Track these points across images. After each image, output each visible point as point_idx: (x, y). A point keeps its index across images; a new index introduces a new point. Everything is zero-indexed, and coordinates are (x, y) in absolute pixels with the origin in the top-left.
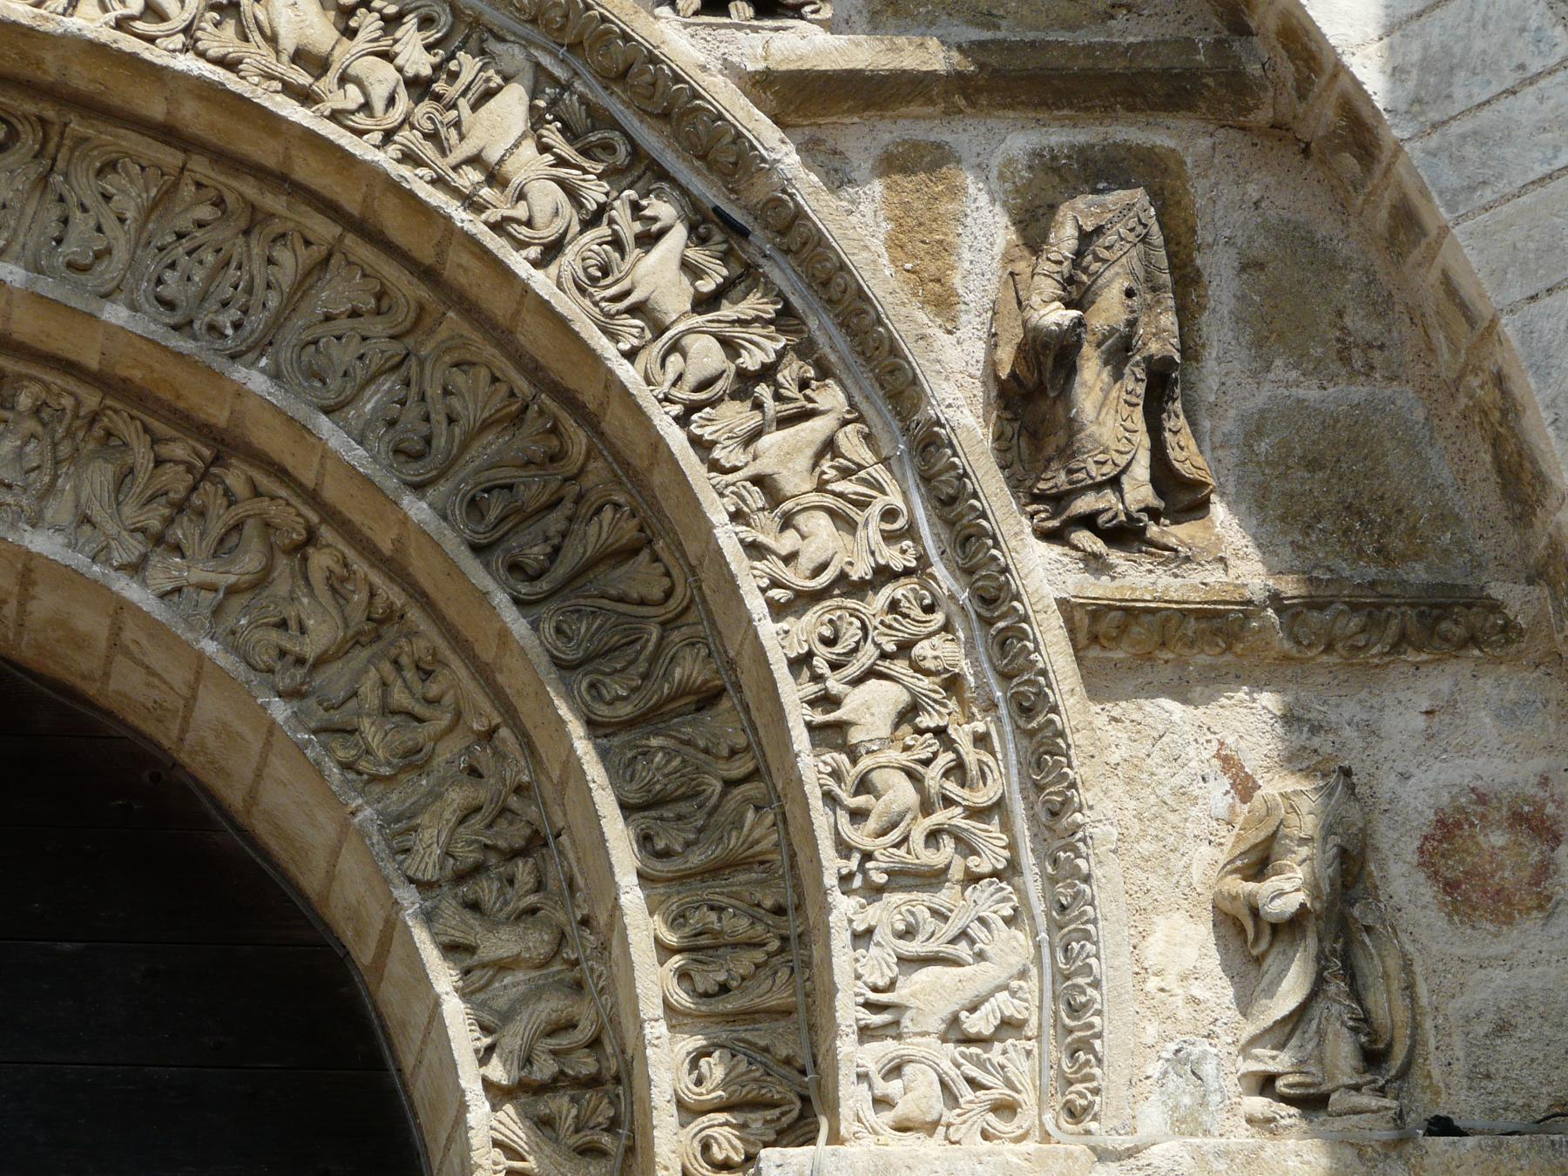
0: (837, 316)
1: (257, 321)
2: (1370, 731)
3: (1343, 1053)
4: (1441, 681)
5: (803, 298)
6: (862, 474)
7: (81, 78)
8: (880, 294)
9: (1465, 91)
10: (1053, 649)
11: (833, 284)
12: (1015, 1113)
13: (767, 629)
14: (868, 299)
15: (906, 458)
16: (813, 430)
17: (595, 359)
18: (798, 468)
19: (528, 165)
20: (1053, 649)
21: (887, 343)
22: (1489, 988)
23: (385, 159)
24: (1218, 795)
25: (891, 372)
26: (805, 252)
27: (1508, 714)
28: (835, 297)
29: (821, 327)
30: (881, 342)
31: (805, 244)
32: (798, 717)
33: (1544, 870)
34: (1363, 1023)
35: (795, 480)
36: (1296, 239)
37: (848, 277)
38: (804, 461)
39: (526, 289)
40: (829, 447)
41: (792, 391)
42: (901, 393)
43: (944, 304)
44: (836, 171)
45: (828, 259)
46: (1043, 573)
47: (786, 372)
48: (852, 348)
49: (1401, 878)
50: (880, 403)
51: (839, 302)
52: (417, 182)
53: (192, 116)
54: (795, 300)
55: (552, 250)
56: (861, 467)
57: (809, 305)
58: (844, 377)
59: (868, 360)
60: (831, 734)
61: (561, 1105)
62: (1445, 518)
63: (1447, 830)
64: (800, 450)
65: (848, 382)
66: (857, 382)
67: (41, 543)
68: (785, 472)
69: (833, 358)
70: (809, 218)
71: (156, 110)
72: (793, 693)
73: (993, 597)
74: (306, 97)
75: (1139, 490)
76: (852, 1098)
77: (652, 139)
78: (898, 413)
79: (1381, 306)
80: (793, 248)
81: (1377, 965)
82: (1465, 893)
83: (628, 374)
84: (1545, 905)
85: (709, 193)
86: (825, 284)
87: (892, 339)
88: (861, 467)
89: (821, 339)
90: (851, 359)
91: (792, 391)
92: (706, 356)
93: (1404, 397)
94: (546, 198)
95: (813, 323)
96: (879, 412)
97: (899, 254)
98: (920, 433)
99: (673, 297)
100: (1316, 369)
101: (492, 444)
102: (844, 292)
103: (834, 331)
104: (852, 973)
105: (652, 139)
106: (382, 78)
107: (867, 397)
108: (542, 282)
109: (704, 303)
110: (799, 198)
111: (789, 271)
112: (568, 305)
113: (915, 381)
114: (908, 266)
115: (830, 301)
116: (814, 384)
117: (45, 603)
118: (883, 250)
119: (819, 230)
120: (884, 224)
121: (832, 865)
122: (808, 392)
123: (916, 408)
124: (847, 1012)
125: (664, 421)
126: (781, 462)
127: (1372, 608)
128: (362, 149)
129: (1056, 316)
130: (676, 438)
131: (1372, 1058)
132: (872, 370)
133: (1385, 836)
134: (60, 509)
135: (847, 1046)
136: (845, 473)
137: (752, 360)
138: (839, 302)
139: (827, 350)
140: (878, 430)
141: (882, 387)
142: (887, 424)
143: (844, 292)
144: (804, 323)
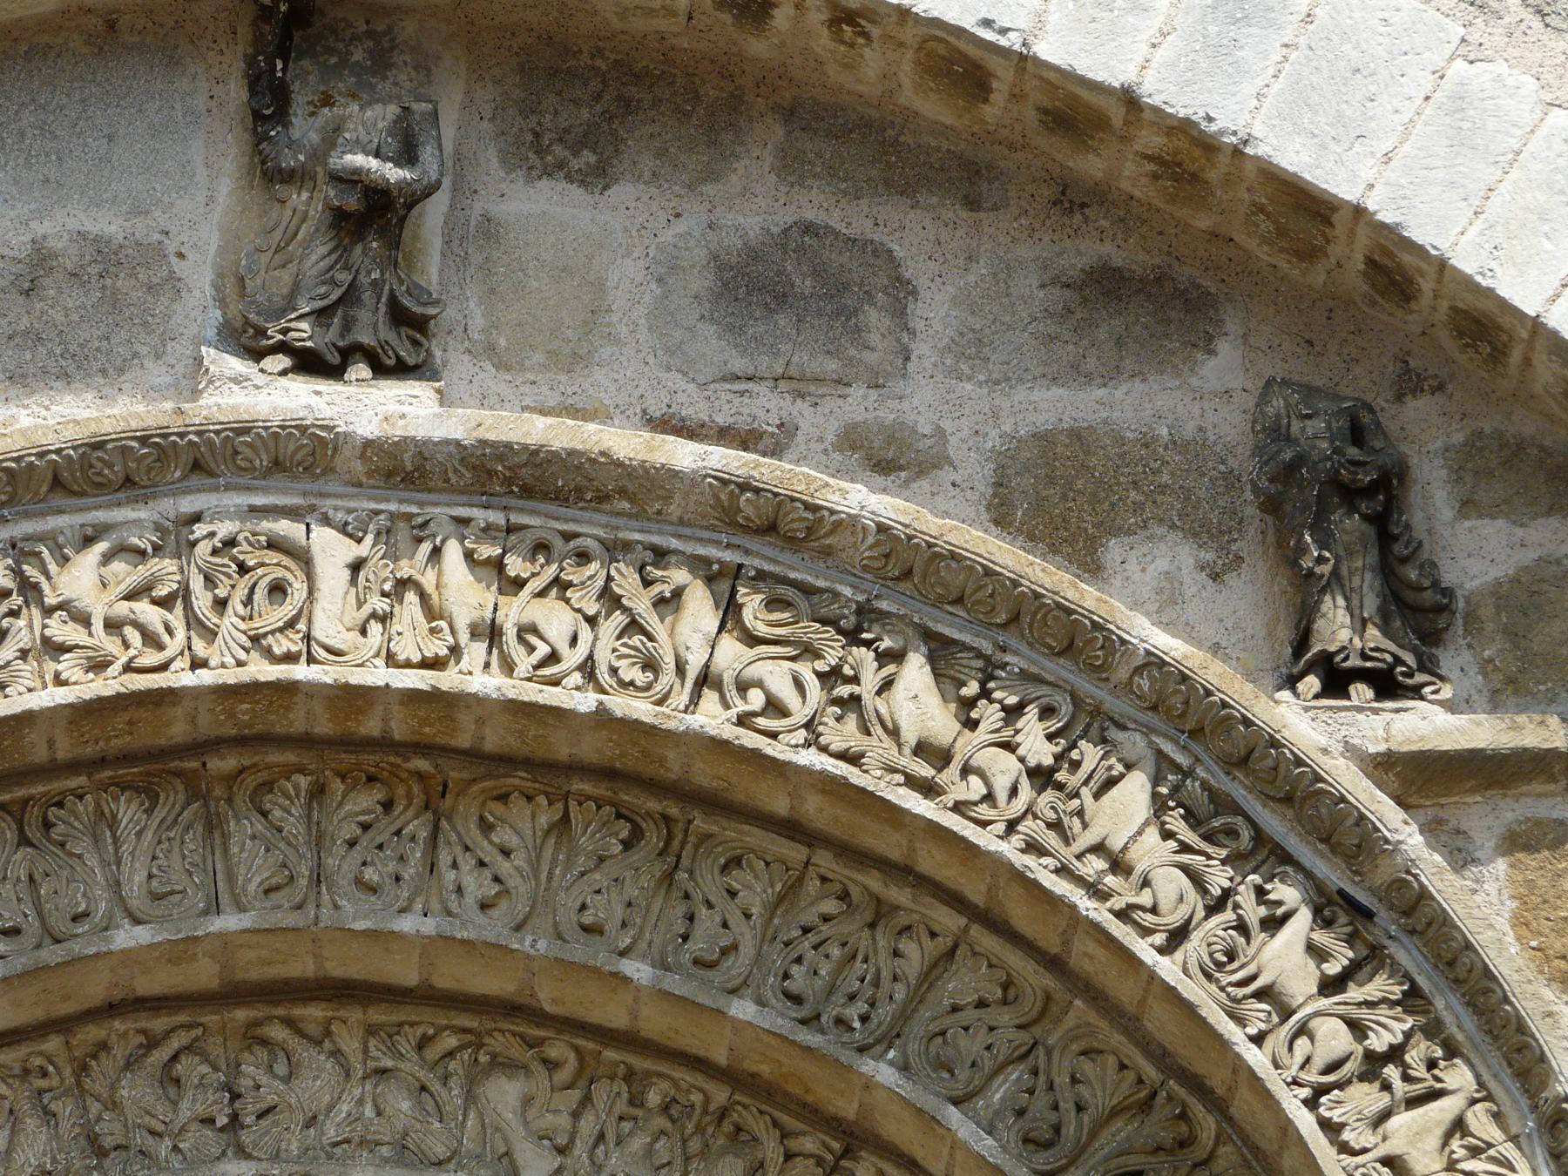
0: (1463, 995)
1: (885, 1012)
5: (1429, 978)
6: (1492, 1152)
7: (705, 775)
8: (1506, 972)
11: (1459, 964)
12: (285, 593)
14: (1494, 978)
15: (1535, 1135)
16: (1442, 1110)
17: (1223, 1044)
18: (1428, 1148)
19: (1151, 852)
21: (1514, 1020)
23: (1009, 849)
25: (1519, 1050)
26: (1431, 933)
28: (1461, 978)
29: (1448, 1007)
30: (1508, 1021)
31: (1429, 924)
37: (1473, 956)
38: (1434, 1141)
39: (1152, 976)
40: (1459, 1126)
41: (1420, 1071)
42: (1529, 1070)
44: (1459, 850)
45: (1453, 939)
47: (1414, 1053)
48: (1479, 1028)
50: (1508, 1081)
51: (1465, 981)
52: (1041, 872)
53: (814, 809)
54: (1421, 980)
55: (1178, 936)
56: (1490, 1146)
57: (1436, 986)
58: (1472, 1056)
59: (1496, 1038)
64: (1428, 1130)
65: (1476, 1061)
66: (1484, 1060)
68: (1414, 1153)
69: (1460, 1037)
70: (1433, 898)
71: (780, 805)
74: (929, 789)
77: (1275, 823)
78: (1527, 1091)
80: (1419, 928)
83: (1256, 1058)
85: (1334, 875)
86: (1451, 964)
87: (1519, 1018)
88: (1490, 1146)
89: (1448, 1019)
90: (1479, 1037)
91: (1420, 1071)
92: (1333, 1038)
94: (1171, 885)
95: (1439, 1003)
96: (1507, 1090)
97: (1524, 931)
98: (1548, 1110)
99: (1300, 980)
101: (1122, 1131)
102: (1470, 971)
103: (1460, 1009)
105: (1275, 823)
106: (1004, 769)
107: (1495, 1076)
108: (1168, 968)
109: (1330, 986)
110: (1423, 879)
111: (1415, 952)
112: (1194, 991)
113: (1542, 1059)
114: (1534, 944)
115: (1456, 981)
116: (1442, 1063)
118: (1507, 928)
119: (1444, 910)
120: (1508, 903)
122: (1436, 1072)
123: (1544, 1085)
125: (1293, 1105)
126: (1411, 1143)
128: (986, 840)
130: (1305, 1121)
132: (1499, 1049)
136: (1475, 1152)
137: (1379, 1042)
138: (1465, 981)
139: (1454, 1029)
140: (1507, 1108)
141: (1510, 1065)
142: (1515, 1101)
143: (1470, 971)
144: (1431, 1004)
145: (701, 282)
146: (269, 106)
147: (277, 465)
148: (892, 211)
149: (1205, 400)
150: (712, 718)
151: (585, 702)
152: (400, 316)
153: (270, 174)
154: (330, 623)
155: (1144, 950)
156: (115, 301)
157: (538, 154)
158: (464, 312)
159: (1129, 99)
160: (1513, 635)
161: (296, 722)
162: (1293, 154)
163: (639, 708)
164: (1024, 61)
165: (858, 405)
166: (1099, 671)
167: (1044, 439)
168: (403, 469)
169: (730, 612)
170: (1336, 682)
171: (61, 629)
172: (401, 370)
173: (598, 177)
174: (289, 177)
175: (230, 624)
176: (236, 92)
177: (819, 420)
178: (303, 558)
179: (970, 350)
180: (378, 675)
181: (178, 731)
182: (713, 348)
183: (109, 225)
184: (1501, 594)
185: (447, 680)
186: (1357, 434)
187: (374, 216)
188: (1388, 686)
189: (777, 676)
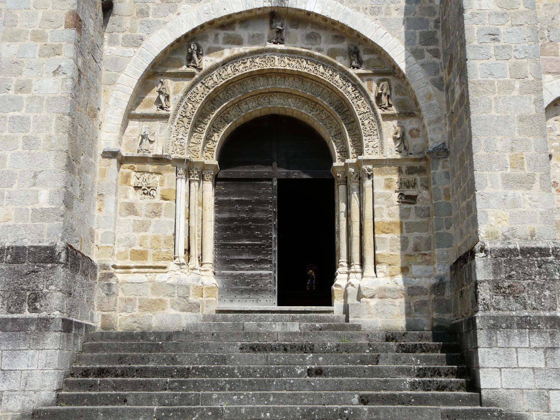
2: (405, 123)
3: (403, 148)
4: (410, 119)
7: (305, 75)
9: (413, 73)
10: (380, 117)
13: (358, 116)
19: (339, 81)
20: (380, 117)
22: (414, 143)
23: (328, 81)
24: (393, 128)
27: (416, 122)
32: (361, 123)
33: (419, 134)
34: (404, 146)
35: (360, 105)
36: (399, 85)
43: (372, 91)
46: (379, 112)
49: (407, 135)
53: (314, 78)
55: (341, 88)
60: (363, 124)
61: (343, 153)
62: (411, 107)
63: (411, 131)
67: (302, 111)
72: (360, 121)
73: (375, 114)
75: (387, 105)
76: (365, 152)
79: (406, 90)
81: (406, 141)
82: (412, 136)
83: (347, 97)
84: (418, 137)
85: (353, 83)
92: (353, 95)
93: (407, 97)
94: (341, 83)
99: (351, 91)
100: (401, 95)
101: (337, 103)
104: (365, 143)
105: (349, 79)
106: (328, 75)
108: (340, 90)
109: (353, 91)
112: (342, 92)
117: (303, 116)
121: (363, 134)
124: (365, 146)
127: (405, 114)
128: (327, 80)
129: (380, 92)
130: (351, 102)
131: (405, 149)
133: (406, 131)
134: (304, 108)
135: (364, 148)
145: (305, 36)
146: (271, 23)
147: (272, 51)
148: (320, 31)
149: (344, 46)
150: (306, 71)
151: (296, 70)
152: (282, 39)
153: (271, 28)
154: (276, 64)
155: (339, 89)
156: (260, 38)
157: (293, 26)
158: (287, 39)
159: (338, 21)
160: (367, 64)
161: (274, 71)
162: (351, 26)
163: (300, 70)
164: (330, 19)
165: (317, 46)
166: (335, 67)
167: (331, 49)
168: (282, 51)
169: (307, 62)
170: (354, 68)
171: (256, 64)
172: (282, 44)
173: (297, 28)
174: (273, 28)
175: (269, 64)
176: (269, 21)
177: (314, 47)
178: (274, 58)
179: (326, 42)
180: (280, 68)
181: (265, 72)
182: (306, 42)
183: (259, 32)
184: (366, 61)
185: (285, 68)
186: (356, 48)
187: (280, 31)
188: (358, 68)
189: (311, 67)
